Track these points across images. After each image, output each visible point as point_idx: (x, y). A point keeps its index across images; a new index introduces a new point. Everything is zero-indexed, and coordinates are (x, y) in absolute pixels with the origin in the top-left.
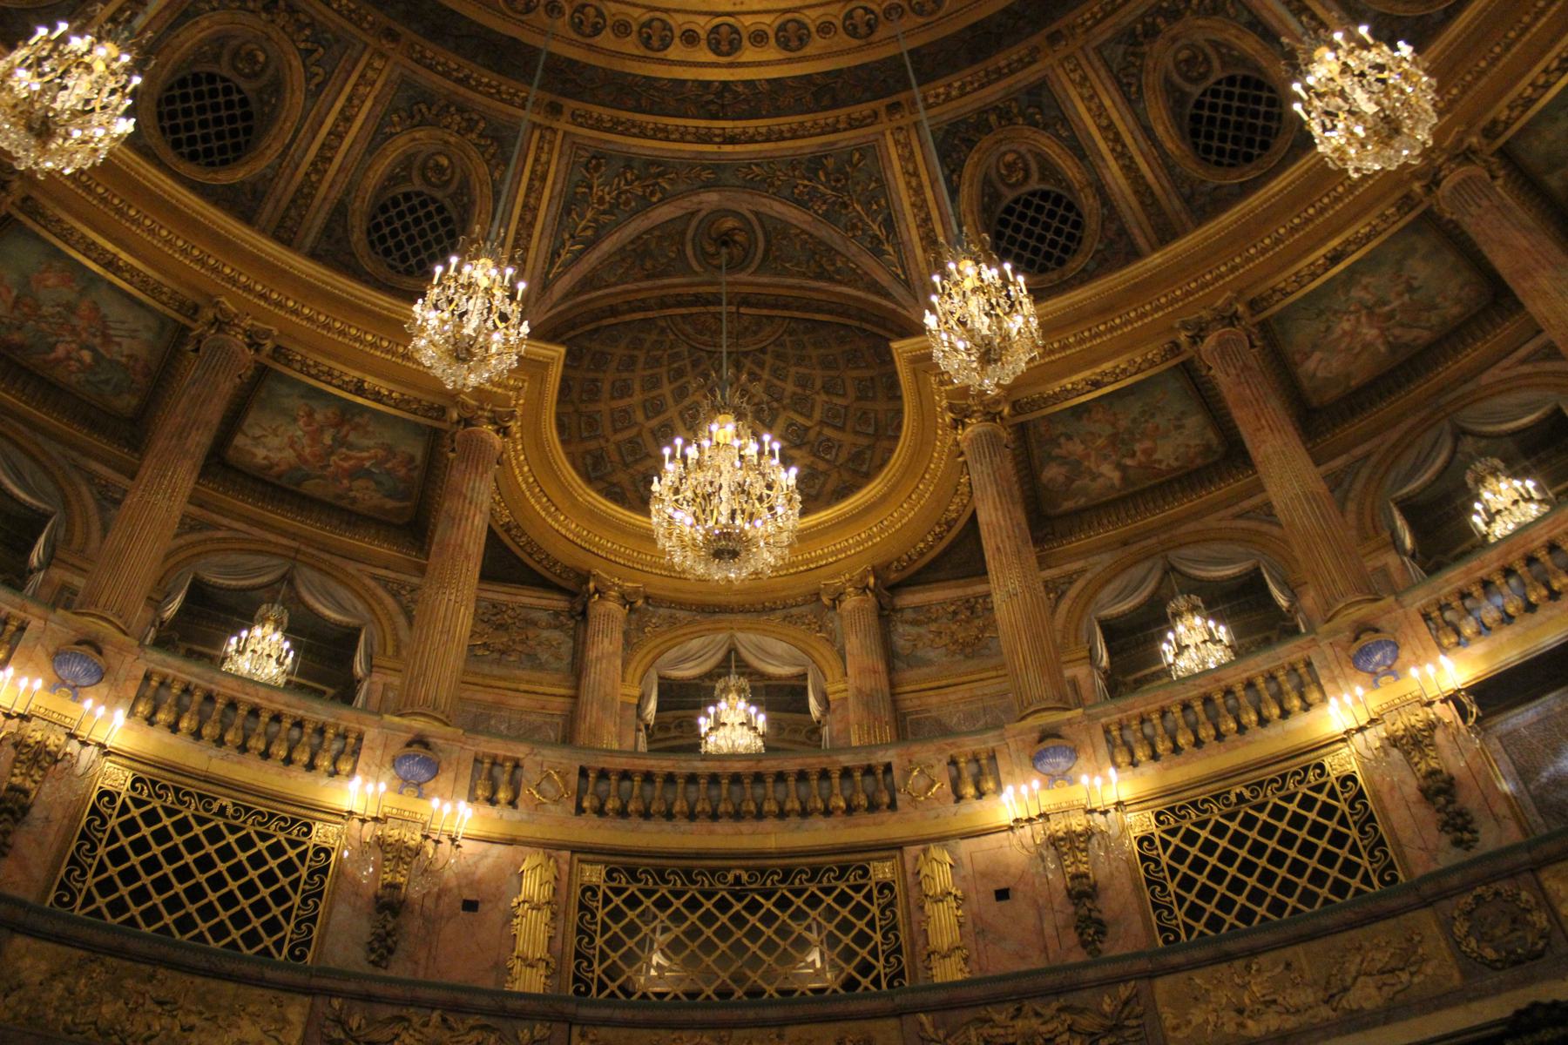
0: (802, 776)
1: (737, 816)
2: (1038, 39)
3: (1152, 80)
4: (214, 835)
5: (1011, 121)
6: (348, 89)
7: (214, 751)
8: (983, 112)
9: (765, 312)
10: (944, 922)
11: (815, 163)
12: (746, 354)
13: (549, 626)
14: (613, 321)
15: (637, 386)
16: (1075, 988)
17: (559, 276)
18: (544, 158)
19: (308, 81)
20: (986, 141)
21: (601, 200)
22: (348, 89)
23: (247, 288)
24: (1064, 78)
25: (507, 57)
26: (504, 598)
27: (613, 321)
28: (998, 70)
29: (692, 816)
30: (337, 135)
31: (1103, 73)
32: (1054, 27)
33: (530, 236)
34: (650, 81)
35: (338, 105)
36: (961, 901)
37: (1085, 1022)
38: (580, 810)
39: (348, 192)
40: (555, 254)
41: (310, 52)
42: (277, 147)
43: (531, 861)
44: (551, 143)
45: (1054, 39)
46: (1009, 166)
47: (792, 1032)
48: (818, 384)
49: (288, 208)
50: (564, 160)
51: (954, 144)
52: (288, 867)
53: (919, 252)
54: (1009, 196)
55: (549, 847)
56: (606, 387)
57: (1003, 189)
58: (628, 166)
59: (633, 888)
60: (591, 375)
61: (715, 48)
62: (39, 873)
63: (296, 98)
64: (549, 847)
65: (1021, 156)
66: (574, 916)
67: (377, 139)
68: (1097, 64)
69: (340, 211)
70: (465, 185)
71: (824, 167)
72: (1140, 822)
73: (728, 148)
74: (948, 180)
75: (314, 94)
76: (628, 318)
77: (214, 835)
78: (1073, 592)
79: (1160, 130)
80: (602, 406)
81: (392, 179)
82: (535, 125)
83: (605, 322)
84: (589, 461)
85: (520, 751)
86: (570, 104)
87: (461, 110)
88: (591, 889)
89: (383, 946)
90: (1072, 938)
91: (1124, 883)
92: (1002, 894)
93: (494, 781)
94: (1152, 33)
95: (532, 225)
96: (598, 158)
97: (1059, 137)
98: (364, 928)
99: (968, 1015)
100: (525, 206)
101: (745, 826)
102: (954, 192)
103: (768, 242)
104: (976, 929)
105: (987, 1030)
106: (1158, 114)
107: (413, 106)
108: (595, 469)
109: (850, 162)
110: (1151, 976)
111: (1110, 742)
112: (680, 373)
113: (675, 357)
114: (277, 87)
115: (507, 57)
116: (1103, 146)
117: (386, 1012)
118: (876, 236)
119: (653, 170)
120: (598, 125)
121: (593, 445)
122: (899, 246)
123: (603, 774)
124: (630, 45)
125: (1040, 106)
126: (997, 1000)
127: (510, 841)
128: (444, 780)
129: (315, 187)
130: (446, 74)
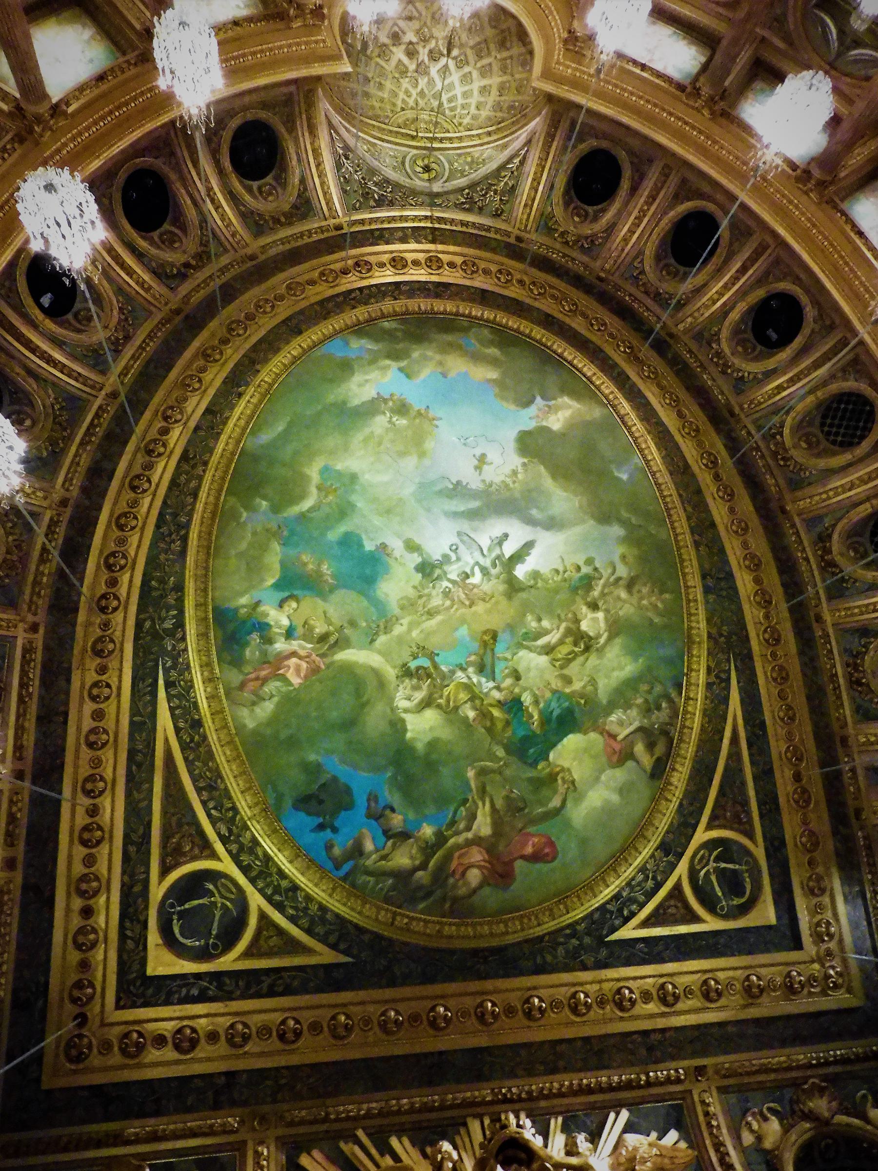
2: (262, 258)
3: (195, 232)
5: (273, 218)
6: (624, 255)
8: (290, 224)
9: (403, 131)
11: (381, 203)
12: (412, 108)
14: (490, 129)
15: (476, 93)
18: (525, 217)
19: (642, 262)
20: (286, 207)
21: (496, 192)
22: (624, 255)
23: (693, 128)
24: (245, 237)
25: (544, 264)
27: (490, 129)
28: (283, 244)
30: (631, 232)
31: (223, 238)
32: (254, 263)
33: (535, 173)
34: (470, 246)
35: (629, 246)
40: (522, 163)
41: (640, 273)
42: (663, 223)
44: (521, 223)
45: (252, 258)
46: (270, 194)
48: (372, 83)
49: (662, 188)
50: (514, 215)
51: (304, 207)
53: (323, 146)
54: (269, 179)
56: (495, 92)
57: (271, 181)
58: (481, 209)
60: (503, 98)
61: (439, 260)
63: (650, 250)
65: (265, 199)
67: (611, 229)
68: (226, 243)
69: (634, 189)
70: (567, 204)
71: (375, 200)
73: (429, 214)
74: (305, 189)
75: (641, 253)
76: (480, 131)
79: (189, 202)
80: (500, 79)
81: (604, 211)
82: (529, 232)
83: (494, 128)
84: (508, 45)
86: (512, 240)
87: (567, 243)
94: (199, 256)
95: (534, 180)
96: (497, 215)
97: (245, 206)
100: (536, 192)
102: (303, 181)
103: (403, 163)
106: (191, 213)
107: (591, 246)
108: (505, 38)
109: (361, 203)
112: (450, 101)
113: (452, 109)
114: (658, 258)
115: (544, 264)
116: (220, 196)
118: (347, 158)
119: (467, 206)
120: (497, 231)
121: (505, 54)
122: (334, 153)
124: (482, 265)
125: (257, 224)
129: (646, 203)
130: (573, 259)
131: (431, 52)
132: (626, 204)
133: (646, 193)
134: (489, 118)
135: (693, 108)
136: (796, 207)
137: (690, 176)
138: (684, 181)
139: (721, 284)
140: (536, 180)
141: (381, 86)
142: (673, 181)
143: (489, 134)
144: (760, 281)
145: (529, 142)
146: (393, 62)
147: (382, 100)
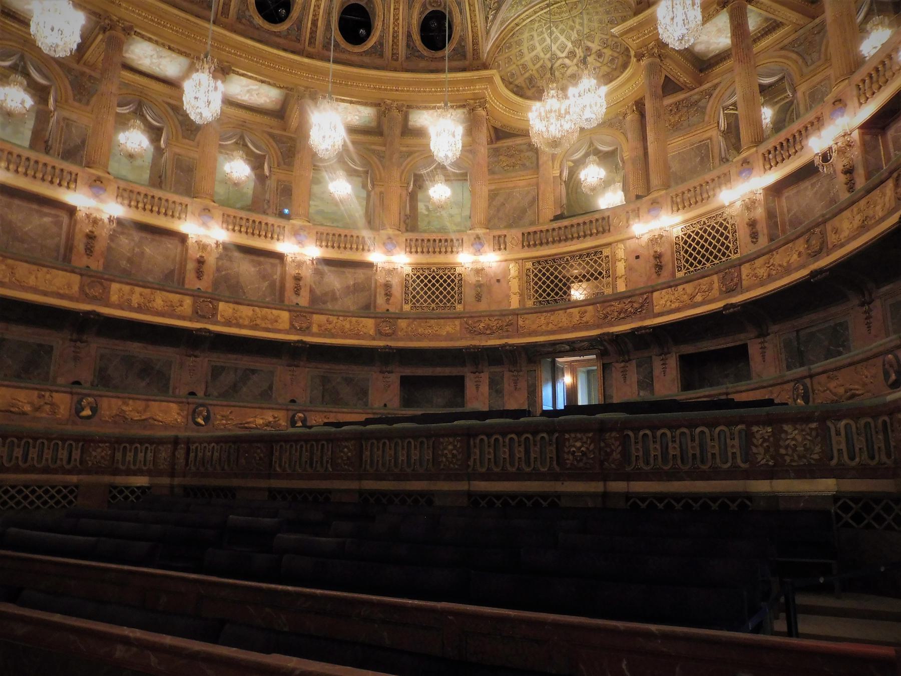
0: (585, 223)
1: (566, 240)
4: (434, 277)
7: (428, 256)
10: (621, 267)
13: (527, 151)
15: (537, 45)
16: (634, 296)
17: (491, 27)
26: (511, 144)
29: (554, 242)
36: (626, 261)
37: (636, 305)
38: (523, 246)
39: (409, 28)
42: (380, 24)
43: (512, 266)
47: (568, 311)
52: (453, 281)
55: (516, 260)
56: (525, 51)
59: (540, 267)
62: (400, 298)
64: (516, 260)
66: (525, 278)
69: (409, 36)
72: (677, 231)
77: (434, 277)
78: (714, 95)
84: (527, 81)
85: (505, 232)
88: (529, 270)
89: (478, 298)
90: (653, 270)
91: (669, 253)
92: (637, 257)
93: (500, 243)
95: (474, 11)
98: (473, 293)
99: (608, 304)
101: (568, 243)
104: (629, 269)
105: (612, 308)
110: (652, 292)
111: (672, 202)
117: (476, 320)
121: (527, 75)
123: (529, 233)
126: (615, 300)
127: (506, 260)
128: (486, 247)
131: (575, 56)
132: (409, 25)
133: (400, 38)
134: (522, 34)
135: (397, 100)
136: (308, 77)
137: (378, 61)
138: (381, 56)
139: (322, 6)
140: (472, 11)
141: (601, 22)
142: (388, 52)
143: (517, 25)
144: (300, 22)
145: (488, 33)
146: (597, 40)
147: (597, 13)
